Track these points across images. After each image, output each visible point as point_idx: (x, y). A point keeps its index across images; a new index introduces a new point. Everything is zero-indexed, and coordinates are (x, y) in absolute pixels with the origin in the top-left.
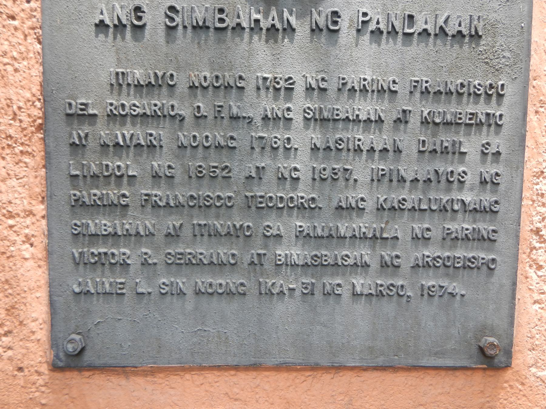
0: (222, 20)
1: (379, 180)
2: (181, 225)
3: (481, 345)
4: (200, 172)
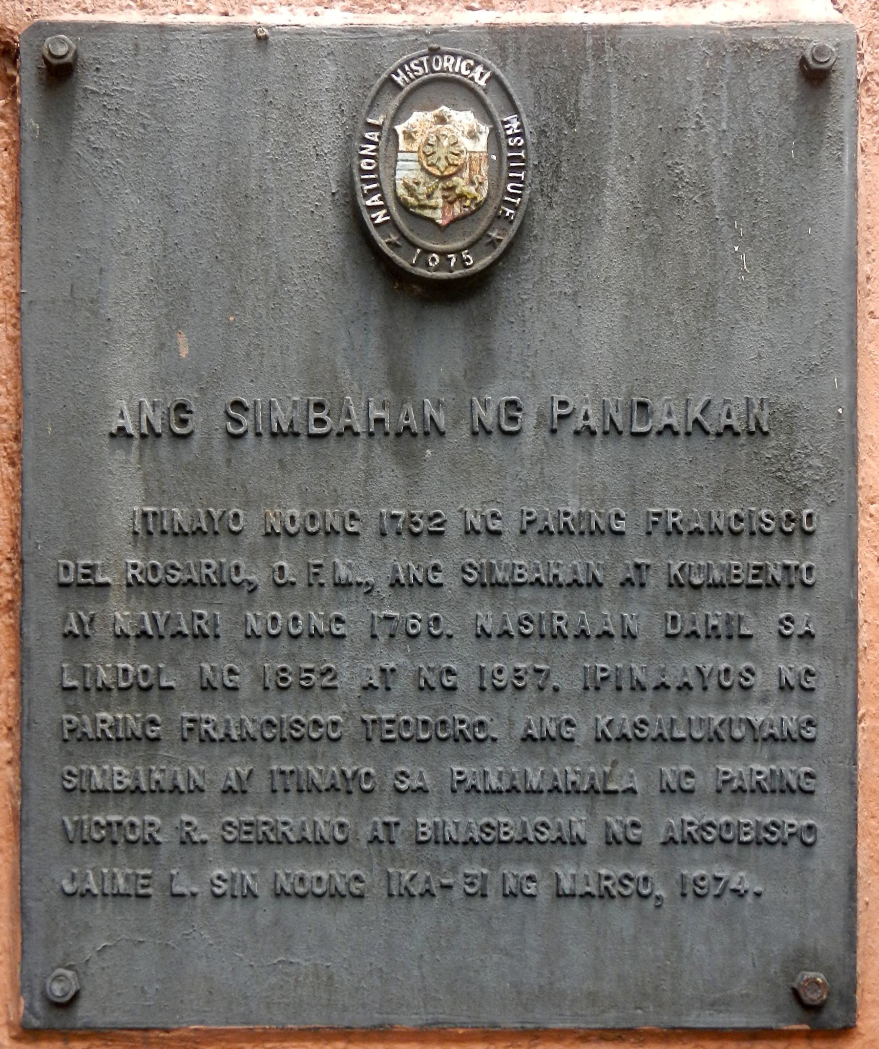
0: (320, 422)
1: (597, 689)
2: (251, 772)
3: (795, 986)
4: (284, 679)
